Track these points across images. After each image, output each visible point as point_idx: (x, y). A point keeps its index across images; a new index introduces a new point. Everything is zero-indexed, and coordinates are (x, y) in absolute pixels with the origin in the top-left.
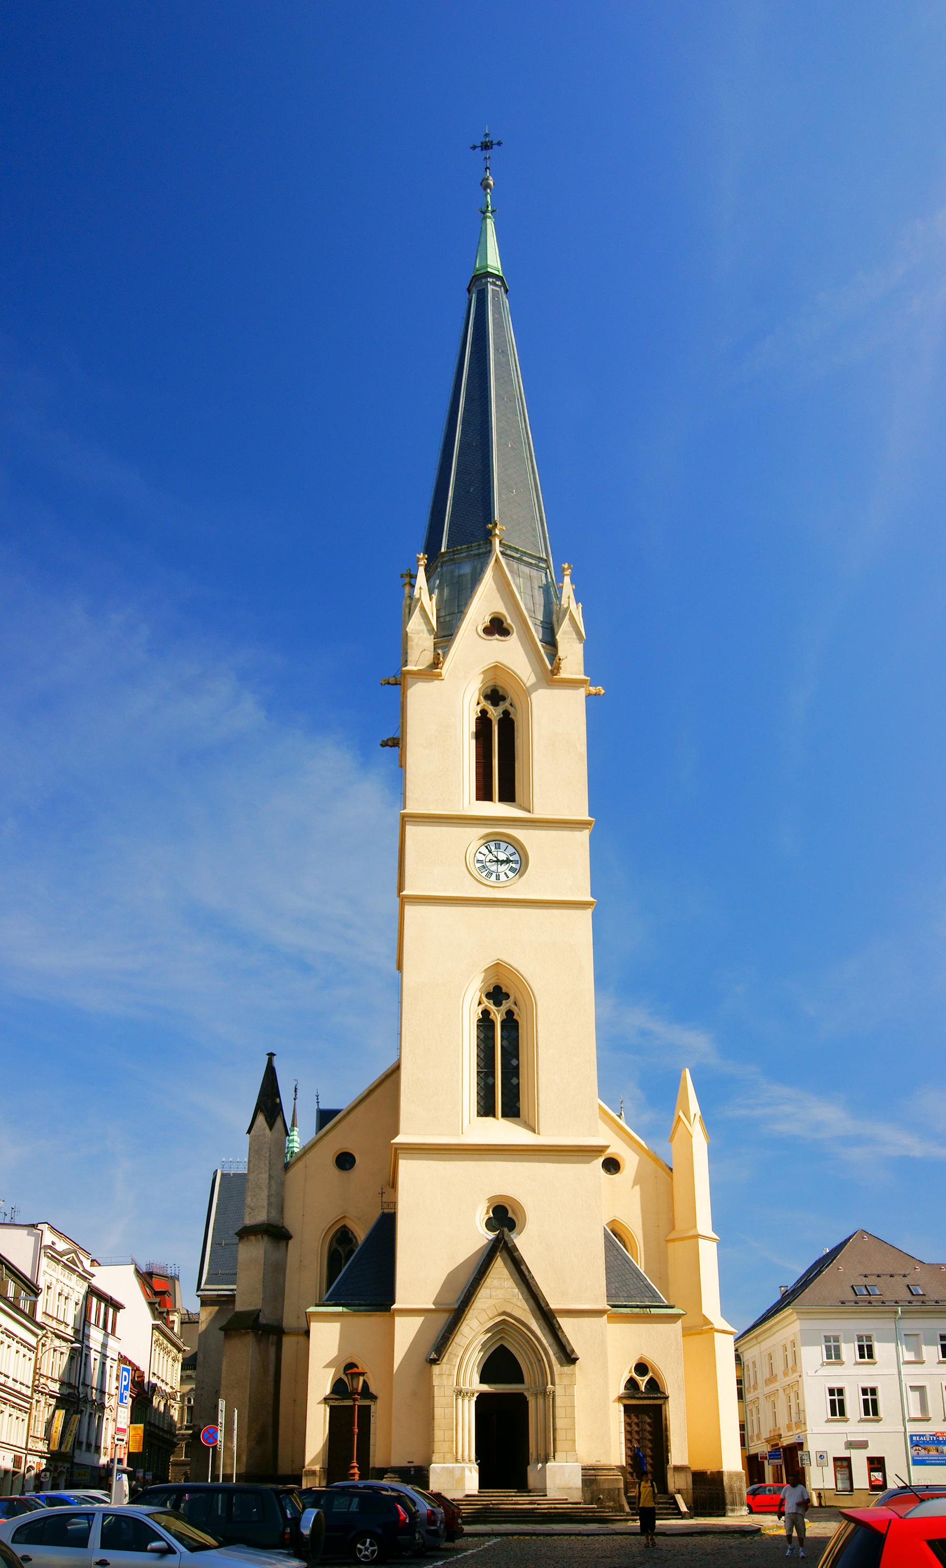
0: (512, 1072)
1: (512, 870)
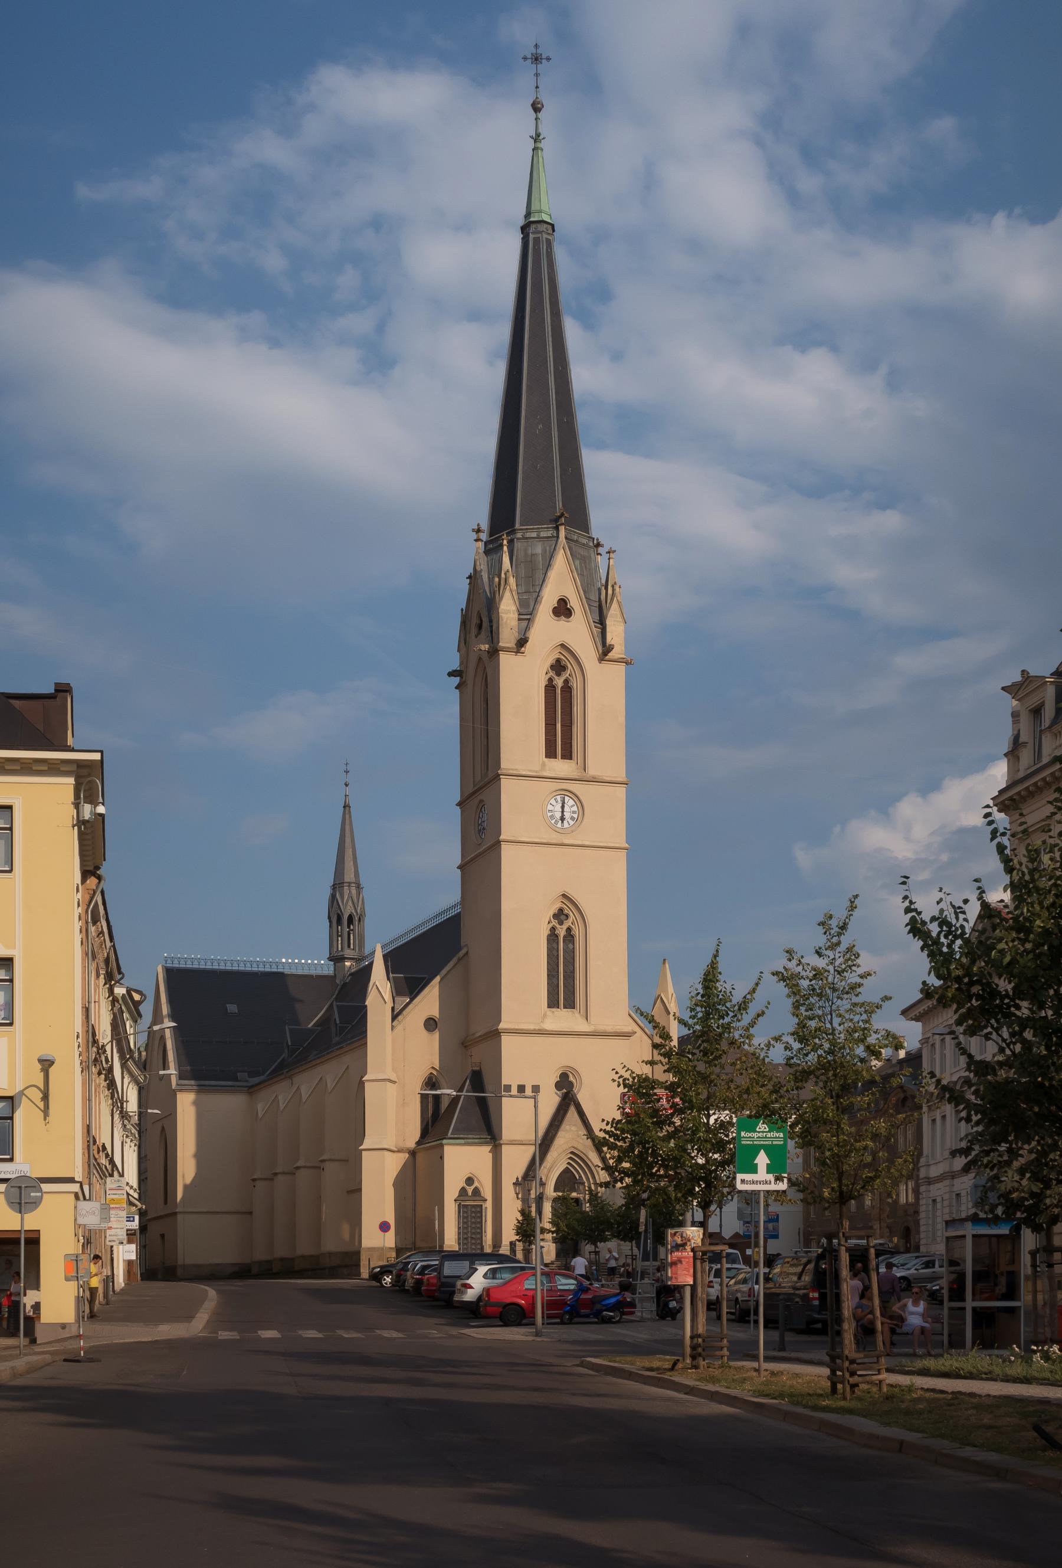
0: (570, 976)
1: (572, 818)
